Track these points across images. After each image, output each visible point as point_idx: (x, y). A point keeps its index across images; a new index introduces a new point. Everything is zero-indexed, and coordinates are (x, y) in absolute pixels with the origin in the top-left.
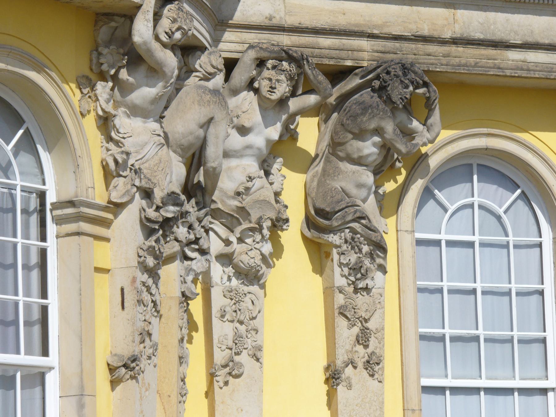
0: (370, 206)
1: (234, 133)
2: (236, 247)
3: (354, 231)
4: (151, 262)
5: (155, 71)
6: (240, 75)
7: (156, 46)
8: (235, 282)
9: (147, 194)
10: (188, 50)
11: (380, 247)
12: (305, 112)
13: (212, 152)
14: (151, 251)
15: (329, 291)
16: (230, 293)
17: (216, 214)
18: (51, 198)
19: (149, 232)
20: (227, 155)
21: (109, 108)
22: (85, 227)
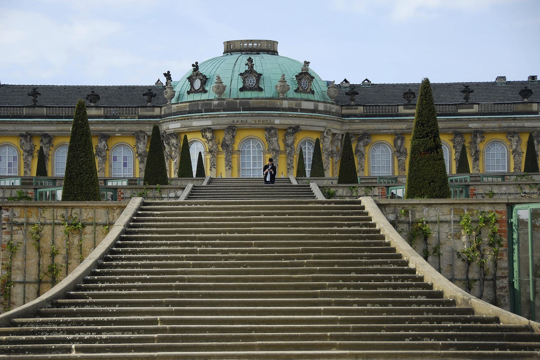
11: (363, 155)
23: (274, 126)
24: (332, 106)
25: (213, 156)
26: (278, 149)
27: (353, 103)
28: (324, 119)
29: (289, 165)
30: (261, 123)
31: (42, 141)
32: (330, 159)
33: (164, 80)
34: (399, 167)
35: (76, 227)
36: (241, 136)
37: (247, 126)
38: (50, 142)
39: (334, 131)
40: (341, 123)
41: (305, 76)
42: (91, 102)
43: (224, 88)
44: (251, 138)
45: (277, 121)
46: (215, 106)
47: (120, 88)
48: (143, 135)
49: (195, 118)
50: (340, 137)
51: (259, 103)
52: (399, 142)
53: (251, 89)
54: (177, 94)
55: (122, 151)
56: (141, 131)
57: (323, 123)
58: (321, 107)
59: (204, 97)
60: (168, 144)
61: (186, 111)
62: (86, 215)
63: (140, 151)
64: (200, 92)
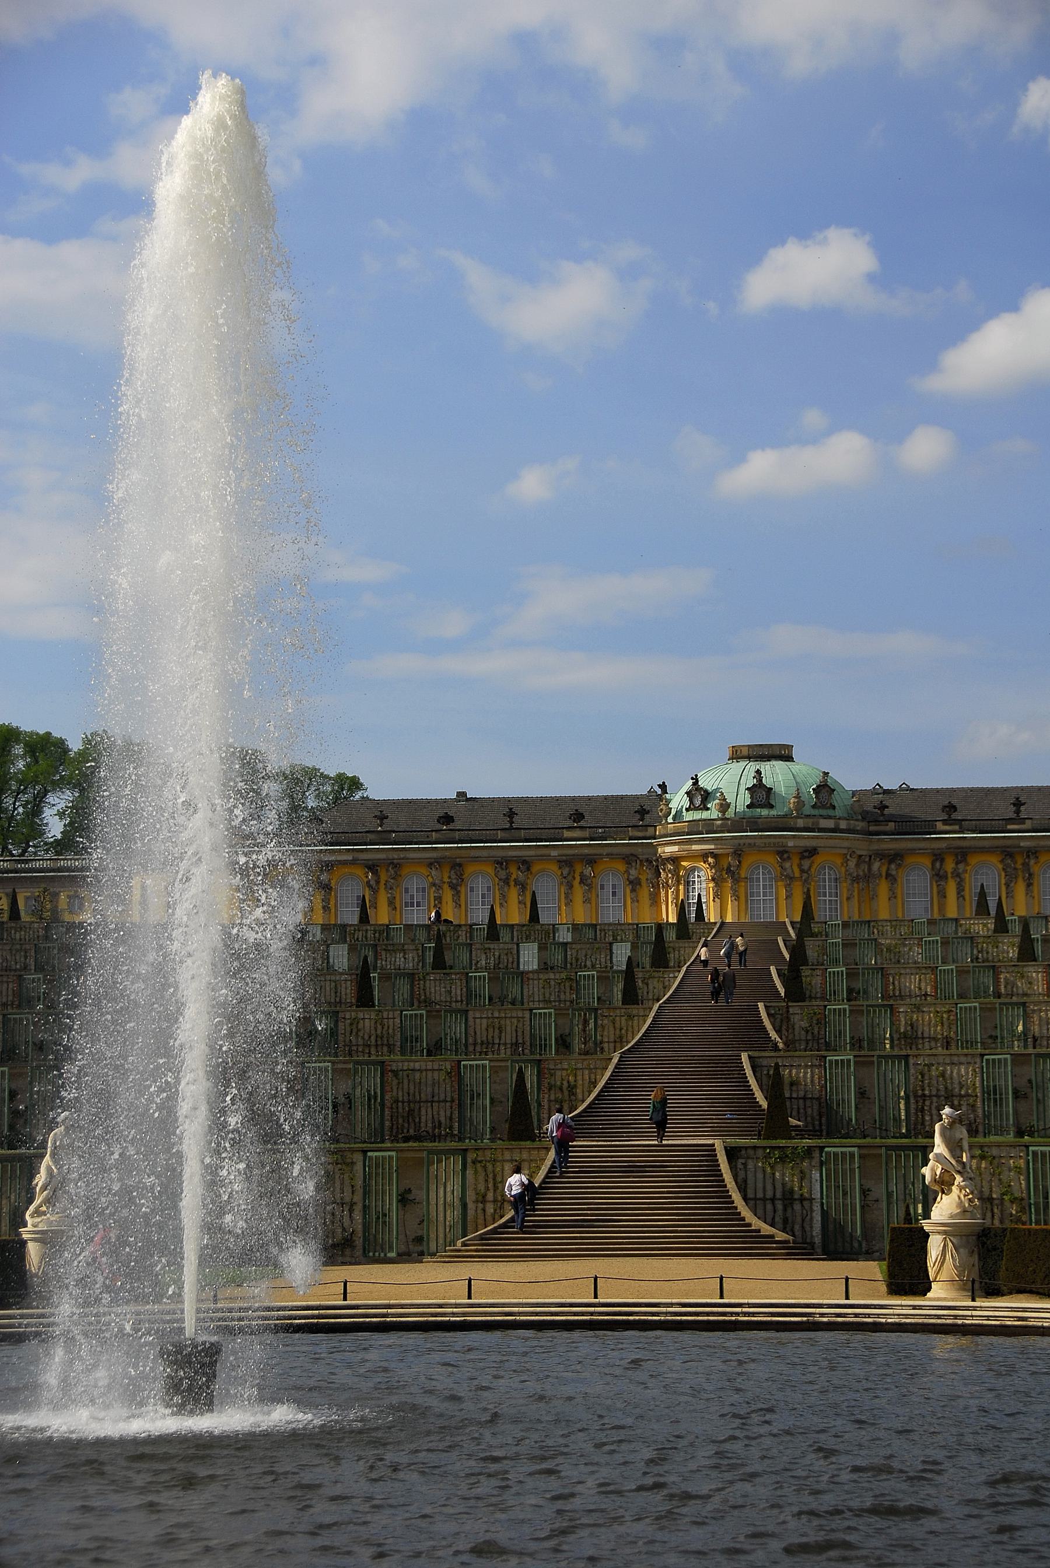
24: (857, 823)
25: (717, 885)
31: (519, 868)
32: (856, 885)
33: (659, 791)
34: (938, 893)
35: (630, 1017)
36: (748, 861)
38: (528, 869)
39: (859, 853)
41: (825, 788)
42: (574, 821)
43: (729, 805)
46: (718, 826)
47: (606, 798)
50: (867, 859)
52: (938, 865)
53: (761, 806)
54: (673, 812)
57: (846, 844)
58: (843, 825)
59: (705, 815)
60: (664, 870)
62: (635, 1012)
63: (631, 877)
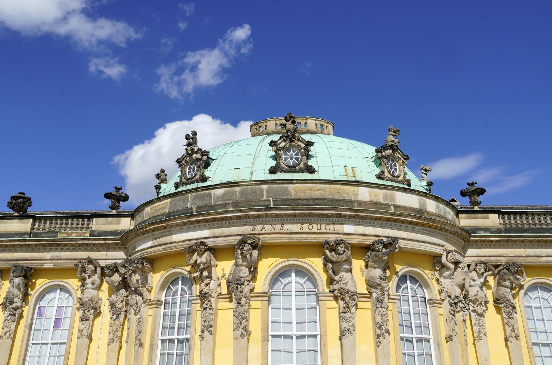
0: (510, 297)
1: (472, 281)
2: (476, 308)
3: (506, 303)
4: (453, 313)
5: (448, 269)
6: (471, 268)
7: (448, 263)
8: (477, 317)
9: (450, 297)
10: (457, 263)
11: (514, 308)
12: (490, 275)
13: (467, 286)
14: (452, 310)
15: (503, 319)
16: (476, 319)
17: (470, 300)
18: (427, 299)
19: (451, 306)
20: (470, 286)
21: (439, 277)
22: (435, 305)
23: (342, 237)
24: (448, 209)
26: (352, 290)
27: (476, 208)
28: (441, 229)
29: (378, 326)
30: (314, 230)
37: (284, 238)
40: (463, 243)
44: (293, 265)
45: (349, 228)
46: (218, 198)
48: (91, 267)
49: (178, 225)
50: (466, 269)
51: (310, 189)
53: (292, 169)
55: (57, 296)
56: (90, 261)
61: (162, 215)
64: (197, 181)
